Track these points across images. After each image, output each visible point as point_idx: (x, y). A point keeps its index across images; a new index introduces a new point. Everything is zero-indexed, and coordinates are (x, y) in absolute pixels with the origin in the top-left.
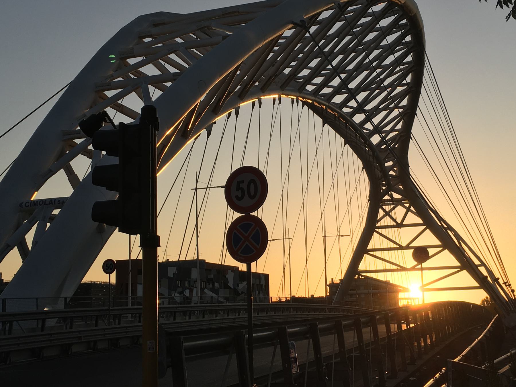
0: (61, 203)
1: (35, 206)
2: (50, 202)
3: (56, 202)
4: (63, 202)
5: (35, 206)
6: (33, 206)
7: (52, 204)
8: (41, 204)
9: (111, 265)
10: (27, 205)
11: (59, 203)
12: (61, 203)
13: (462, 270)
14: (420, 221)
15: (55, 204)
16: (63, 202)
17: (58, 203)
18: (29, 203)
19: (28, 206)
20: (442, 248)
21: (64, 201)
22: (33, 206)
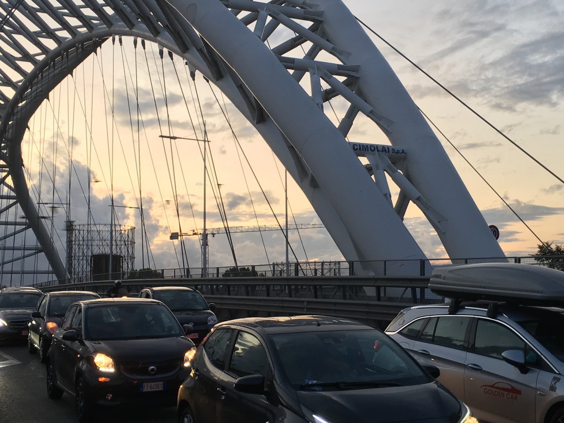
0: (396, 153)
1: (365, 150)
2: (383, 149)
3: (390, 150)
4: (398, 152)
5: (365, 150)
6: (363, 150)
7: (386, 152)
8: (373, 149)
9: (495, 232)
10: (355, 148)
11: (394, 153)
12: (396, 153)
13: (38, 251)
14: (13, 194)
15: (388, 152)
16: (398, 152)
17: (393, 152)
18: (357, 146)
19: (357, 149)
20: (24, 227)
21: (399, 151)
22: (363, 150)
